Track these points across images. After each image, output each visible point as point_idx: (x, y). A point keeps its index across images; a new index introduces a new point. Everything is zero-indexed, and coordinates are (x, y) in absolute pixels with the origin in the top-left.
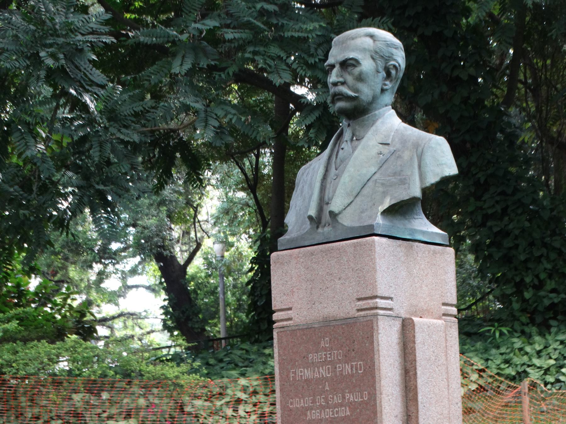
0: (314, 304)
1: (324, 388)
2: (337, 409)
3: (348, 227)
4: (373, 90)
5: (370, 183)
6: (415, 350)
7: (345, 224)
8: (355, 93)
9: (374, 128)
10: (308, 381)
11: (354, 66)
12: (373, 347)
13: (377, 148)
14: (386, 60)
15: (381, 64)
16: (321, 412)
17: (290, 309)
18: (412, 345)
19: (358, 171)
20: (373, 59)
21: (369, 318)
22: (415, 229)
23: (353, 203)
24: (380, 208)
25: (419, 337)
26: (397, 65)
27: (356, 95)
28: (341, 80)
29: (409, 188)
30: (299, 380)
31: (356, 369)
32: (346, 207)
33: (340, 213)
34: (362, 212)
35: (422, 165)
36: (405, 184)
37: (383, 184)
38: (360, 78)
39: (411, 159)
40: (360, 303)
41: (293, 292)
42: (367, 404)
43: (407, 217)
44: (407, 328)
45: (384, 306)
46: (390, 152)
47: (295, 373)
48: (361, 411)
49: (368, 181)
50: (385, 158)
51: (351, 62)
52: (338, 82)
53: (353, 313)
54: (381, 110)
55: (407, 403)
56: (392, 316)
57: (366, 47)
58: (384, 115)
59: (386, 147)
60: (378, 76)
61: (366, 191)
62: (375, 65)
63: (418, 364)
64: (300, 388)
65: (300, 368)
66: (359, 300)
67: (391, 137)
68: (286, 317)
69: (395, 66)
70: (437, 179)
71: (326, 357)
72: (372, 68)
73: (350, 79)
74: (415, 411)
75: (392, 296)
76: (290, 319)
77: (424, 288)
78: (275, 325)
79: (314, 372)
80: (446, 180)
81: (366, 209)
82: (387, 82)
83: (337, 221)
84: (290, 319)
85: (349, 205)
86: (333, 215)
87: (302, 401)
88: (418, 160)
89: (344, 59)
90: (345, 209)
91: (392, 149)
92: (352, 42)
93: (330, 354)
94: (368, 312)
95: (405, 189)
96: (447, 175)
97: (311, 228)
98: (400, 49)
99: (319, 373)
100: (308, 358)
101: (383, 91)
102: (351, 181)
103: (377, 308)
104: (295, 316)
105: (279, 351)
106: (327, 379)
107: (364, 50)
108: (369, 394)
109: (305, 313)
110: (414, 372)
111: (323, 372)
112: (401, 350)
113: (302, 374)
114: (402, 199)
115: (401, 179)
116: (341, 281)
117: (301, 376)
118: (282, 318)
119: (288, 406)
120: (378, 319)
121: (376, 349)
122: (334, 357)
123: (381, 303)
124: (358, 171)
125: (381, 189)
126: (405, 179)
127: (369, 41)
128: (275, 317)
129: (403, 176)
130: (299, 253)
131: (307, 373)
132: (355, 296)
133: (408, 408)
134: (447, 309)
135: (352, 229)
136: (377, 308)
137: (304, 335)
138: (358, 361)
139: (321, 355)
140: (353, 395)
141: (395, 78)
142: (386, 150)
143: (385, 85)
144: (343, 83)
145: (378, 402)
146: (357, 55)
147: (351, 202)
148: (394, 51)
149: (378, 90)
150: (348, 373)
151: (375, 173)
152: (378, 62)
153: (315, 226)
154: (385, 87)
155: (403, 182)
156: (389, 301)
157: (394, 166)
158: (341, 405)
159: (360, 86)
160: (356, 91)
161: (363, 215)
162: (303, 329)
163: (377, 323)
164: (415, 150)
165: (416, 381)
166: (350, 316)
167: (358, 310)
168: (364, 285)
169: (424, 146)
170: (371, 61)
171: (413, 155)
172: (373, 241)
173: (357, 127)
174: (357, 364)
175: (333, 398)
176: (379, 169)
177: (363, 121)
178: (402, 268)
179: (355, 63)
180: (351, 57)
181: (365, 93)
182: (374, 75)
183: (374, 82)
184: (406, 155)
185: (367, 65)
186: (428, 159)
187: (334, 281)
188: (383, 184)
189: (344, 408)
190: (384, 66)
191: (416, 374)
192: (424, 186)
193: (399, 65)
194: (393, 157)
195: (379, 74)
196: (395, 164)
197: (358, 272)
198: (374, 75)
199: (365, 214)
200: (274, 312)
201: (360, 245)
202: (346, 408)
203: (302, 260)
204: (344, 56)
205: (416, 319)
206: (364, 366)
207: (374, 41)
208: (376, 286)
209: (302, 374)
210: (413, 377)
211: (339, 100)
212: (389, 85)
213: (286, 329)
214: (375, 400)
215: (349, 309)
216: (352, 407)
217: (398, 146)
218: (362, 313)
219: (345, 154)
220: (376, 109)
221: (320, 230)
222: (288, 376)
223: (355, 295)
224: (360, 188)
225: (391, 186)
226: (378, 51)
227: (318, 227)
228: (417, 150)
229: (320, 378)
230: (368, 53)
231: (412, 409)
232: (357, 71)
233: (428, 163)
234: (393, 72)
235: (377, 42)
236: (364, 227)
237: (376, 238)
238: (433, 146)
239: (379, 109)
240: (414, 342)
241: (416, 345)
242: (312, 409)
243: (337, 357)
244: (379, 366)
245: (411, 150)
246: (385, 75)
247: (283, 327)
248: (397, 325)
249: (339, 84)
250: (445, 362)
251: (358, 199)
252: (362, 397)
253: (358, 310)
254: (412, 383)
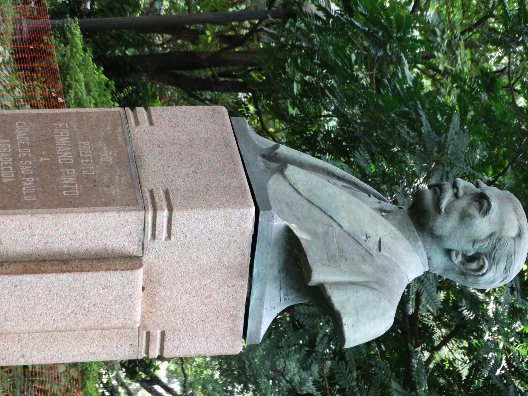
0: (159, 147)
1: (42, 156)
2: (12, 169)
3: (267, 184)
4: (450, 236)
5: (327, 219)
6: (96, 271)
7: (270, 182)
8: (445, 209)
9: (400, 235)
11: (480, 209)
12: (99, 206)
13: (374, 235)
14: (490, 254)
15: (484, 246)
16: (8, 153)
17: (151, 123)
18: (103, 267)
19: (343, 206)
20: (491, 235)
21: (140, 201)
22: (266, 283)
23: (299, 196)
24: (294, 225)
25: (115, 278)
26: (484, 271)
27: (443, 209)
28: (461, 193)
29: (323, 265)
30: (54, 131)
31: (67, 189)
32: (293, 187)
33: (285, 177)
34: (287, 204)
35: (356, 286)
36: (329, 261)
37: (327, 233)
38: (464, 216)
39: (363, 274)
43: (282, 275)
44: (129, 261)
45: (158, 222)
46: (370, 249)
47: (64, 127)
48: (8, 193)
49: (330, 217)
50: (362, 242)
51: (486, 204)
52: (457, 189)
53: (147, 187)
54: (423, 249)
55: (21, 262)
56: (144, 238)
57: (506, 226)
58: (417, 253)
59: (376, 247)
60: (468, 242)
61: (315, 211)
62: (482, 238)
63: (77, 275)
65: (70, 133)
66: (167, 193)
67: (389, 256)
68: (140, 120)
69: (482, 267)
70: (337, 306)
71: (86, 159)
72: (479, 234)
73: (462, 203)
74: (8, 271)
75: (173, 238)
76: (137, 123)
77: (185, 298)
78: (128, 109)
80: (335, 319)
81: (291, 210)
82: (460, 258)
83: (273, 174)
84: (137, 123)
85: (296, 190)
86: (281, 171)
87: (25, 135)
88: (361, 282)
89: (488, 195)
90: (290, 184)
91: (375, 252)
92: (511, 209)
94: (149, 201)
95: (322, 260)
96: (344, 321)
97: (262, 149)
98: (504, 276)
99: (63, 151)
100: (84, 140)
101: (448, 252)
102: (329, 195)
103: (155, 211)
104: (142, 128)
107: (502, 223)
108: (33, 202)
110: (65, 270)
112: (96, 254)
113: (62, 135)
114: (308, 254)
115: (335, 256)
116: (191, 175)
117: (60, 134)
118: (139, 116)
120: (139, 211)
121: (97, 208)
122: (86, 166)
123: (163, 215)
124: (343, 206)
125: (320, 230)
126: (335, 261)
127: (513, 233)
128: (141, 111)
129: (340, 260)
130: (228, 133)
132: (171, 188)
133: (13, 264)
134: (156, 339)
136: (155, 211)
138: (79, 190)
140: (32, 185)
141: (466, 269)
142: (372, 244)
143: (457, 255)
144: (456, 196)
145: (21, 211)
146: (495, 211)
147: (300, 194)
148: (502, 266)
149: (450, 244)
150: (63, 181)
151: (341, 226)
152: (487, 243)
153: (265, 153)
154: (454, 254)
155: (331, 261)
156: (165, 234)
157: (351, 250)
158: (17, 173)
159: (454, 217)
160: (448, 211)
161: (284, 205)
163: (134, 210)
164: (375, 280)
165: (51, 272)
166: (143, 183)
168: (187, 196)
169: (382, 292)
170: (488, 233)
171: (368, 276)
172: (249, 206)
173: (399, 216)
174: (75, 189)
175: (27, 165)
176: (345, 231)
177: (407, 224)
178: (212, 257)
179: (485, 211)
180: (492, 203)
181: (446, 225)
182: (469, 237)
183: (460, 236)
184: (367, 268)
185: (483, 226)
186: (364, 295)
187: (192, 167)
188: (327, 233)
189: (13, 176)
190: (483, 251)
191: (63, 272)
192: (326, 286)
193: (483, 275)
194: (364, 253)
195: (471, 244)
196: (355, 252)
197: (205, 190)
198: (469, 237)
199: (285, 207)
200: (146, 109)
201: (243, 193)
202: (12, 178)
203: (218, 135)
204: (492, 197)
205: (140, 273)
206: (73, 196)
207: (514, 239)
208: (186, 209)
209: (62, 135)
210: (57, 268)
212: (458, 260)
213: (124, 119)
214: (23, 208)
215: (153, 179)
216: (15, 184)
217: (379, 261)
218: (147, 195)
219: (363, 198)
220: (424, 242)
221: (260, 158)
222: (59, 121)
224: (320, 206)
225: (325, 243)
226: (502, 242)
227: (264, 156)
228: (375, 282)
229: (56, 152)
230: (498, 227)
231: (12, 268)
232: (474, 211)
233: (359, 294)
234: (474, 265)
235: (512, 242)
236: (268, 201)
237: (254, 209)
238: (382, 304)
239: (425, 247)
240: (107, 270)
241: (104, 272)
243: (86, 169)
244: (72, 212)
245: (373, 275)
246: (470, 254)
247: (126, 117)
248: (132, 248)
249: (455, 190)
250: (81, 326)
251: (305, 202)
252: (27, 194)
254: (50, 267)
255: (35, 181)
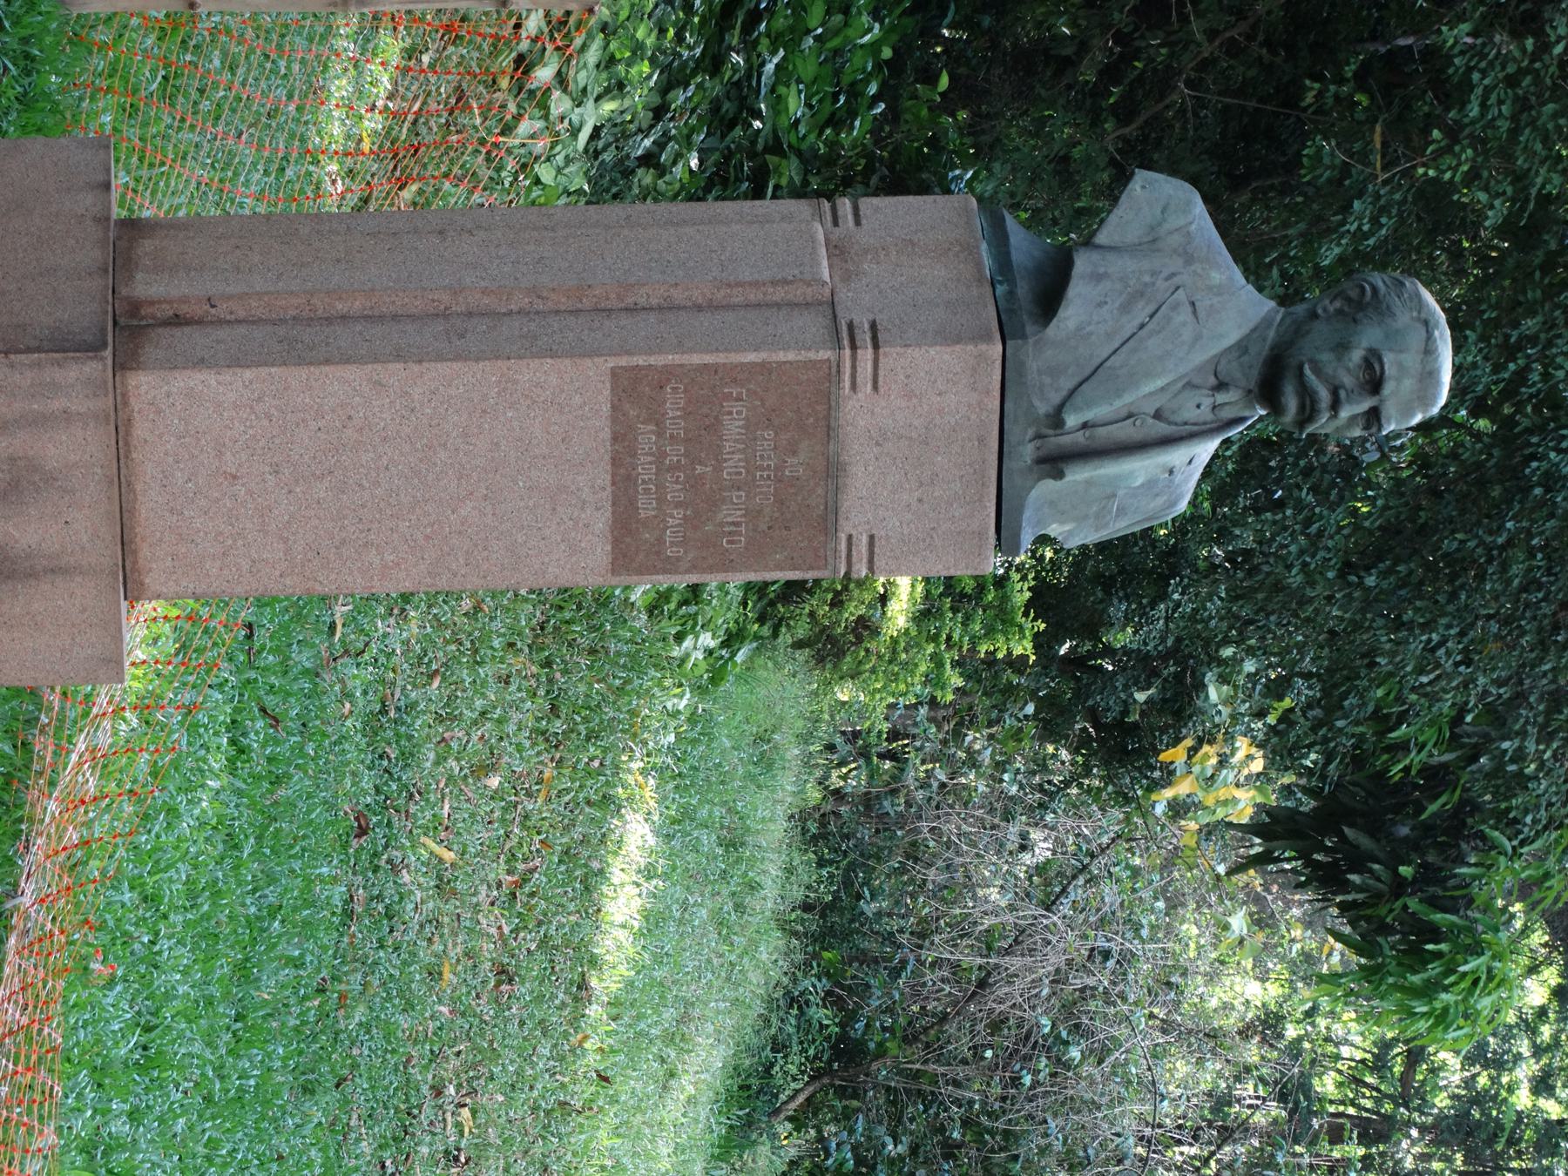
10: (714, 427)
17: (875, 387)
21: (831, 560)
40: (865, 539)
41: (909, 395)
42: (658, 553)
47: (739, 399)
53: (846, 528)
64: (705, 410)
66: (872, 537)
71: (762, 469)
79: (736, 441)
83: (1039, 479)
93: (769, 477)
94: (844, 555)
105: (791, 363)
106: (718, 469)
108: (678, 559)
109: (862, 423)
111: (734, 463)
117: (730, 413)
119: (668, 380)
131: (733, 427)
135: (1020, 510)
137: (817, 420)
139: (769, 458)
158: (661, 500)
162: (828, 417)
166: (841, 521)
167: (850, 537)
175: (677, 482)
203: (974, 417)
211: (1302, 407)
218: (843, 546)
223: (883, 533)
242: (659, 435)
253: (850, 537)
255: (685, 517)
